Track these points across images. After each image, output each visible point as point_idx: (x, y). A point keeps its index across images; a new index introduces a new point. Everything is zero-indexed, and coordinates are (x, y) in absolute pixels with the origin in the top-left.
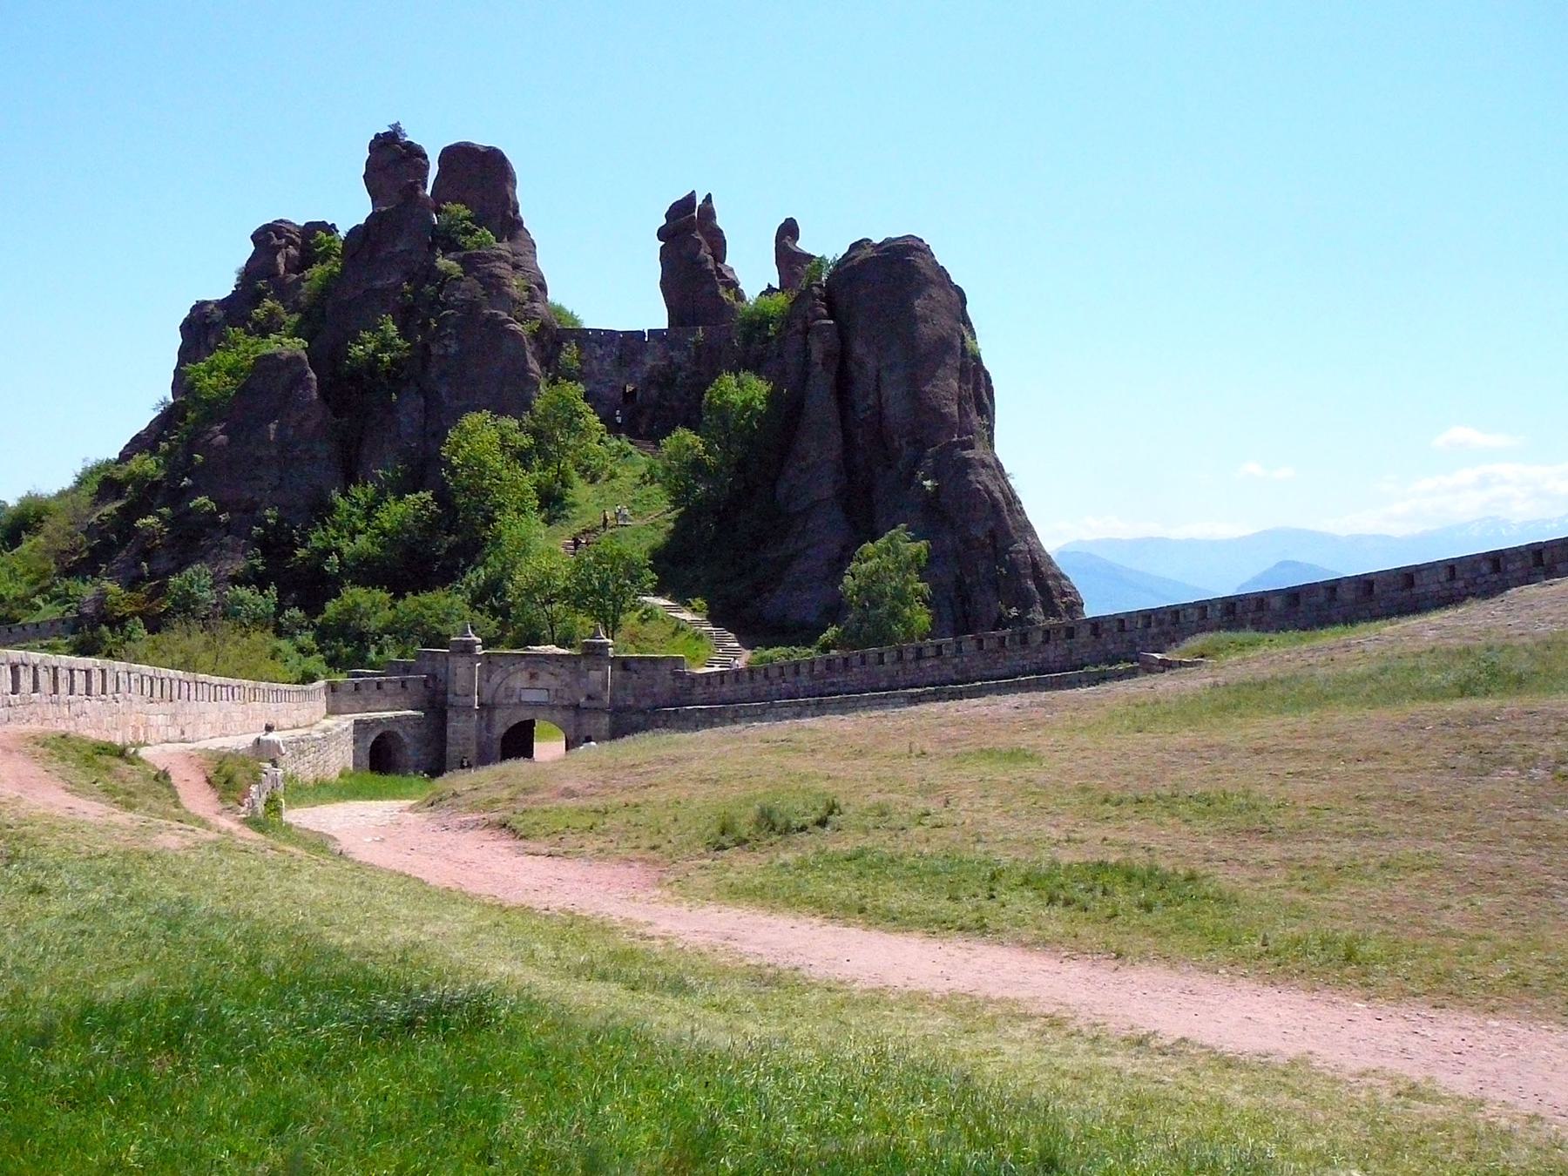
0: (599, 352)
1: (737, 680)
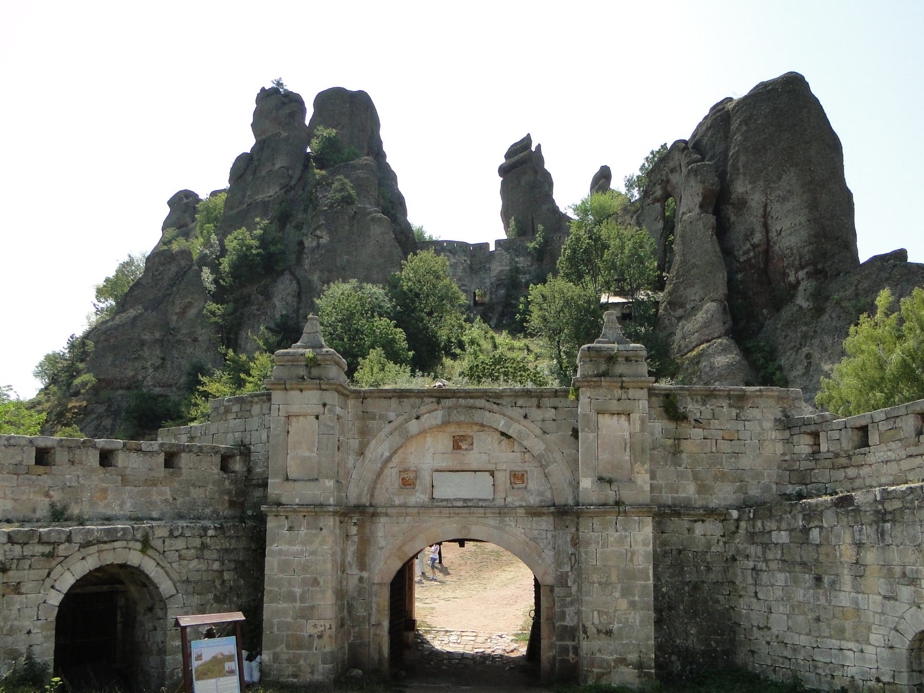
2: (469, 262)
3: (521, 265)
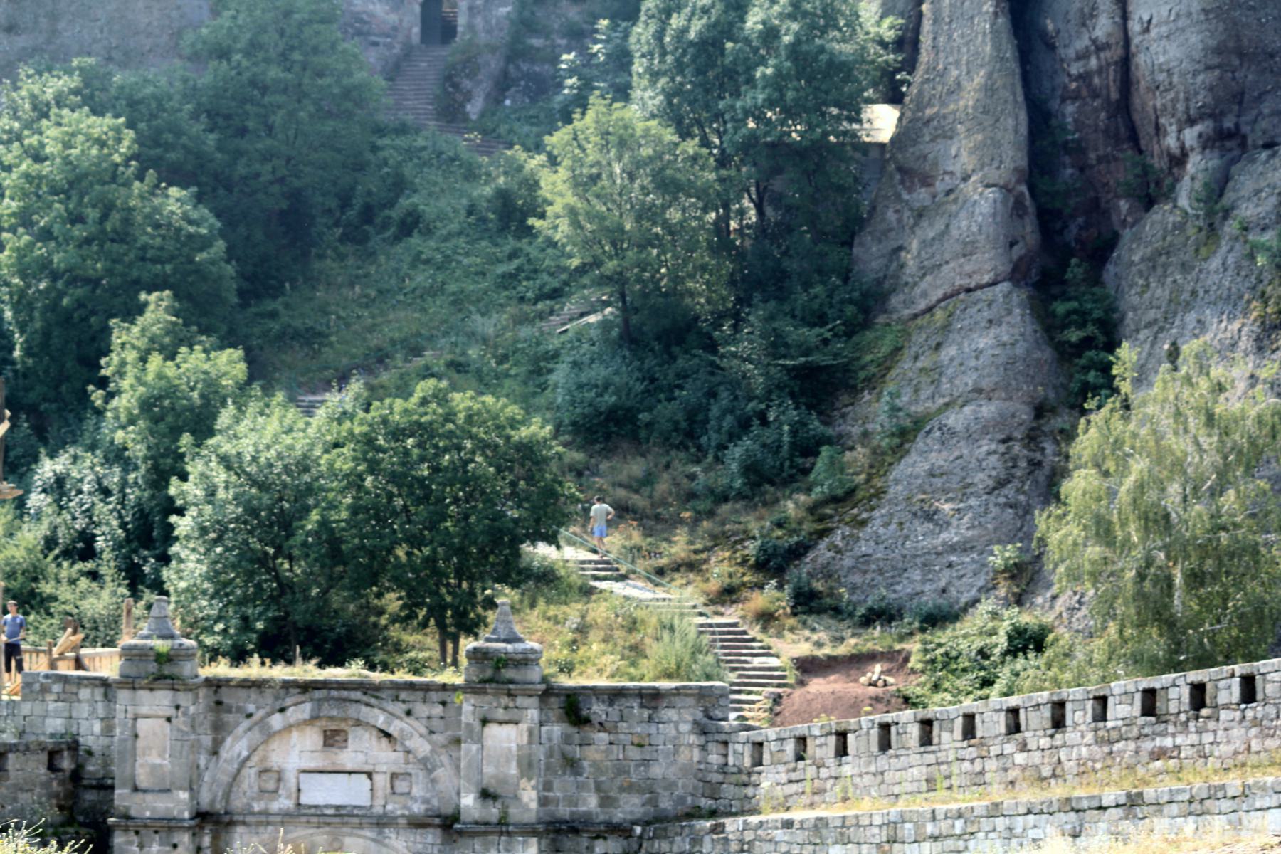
1: (885, 745)
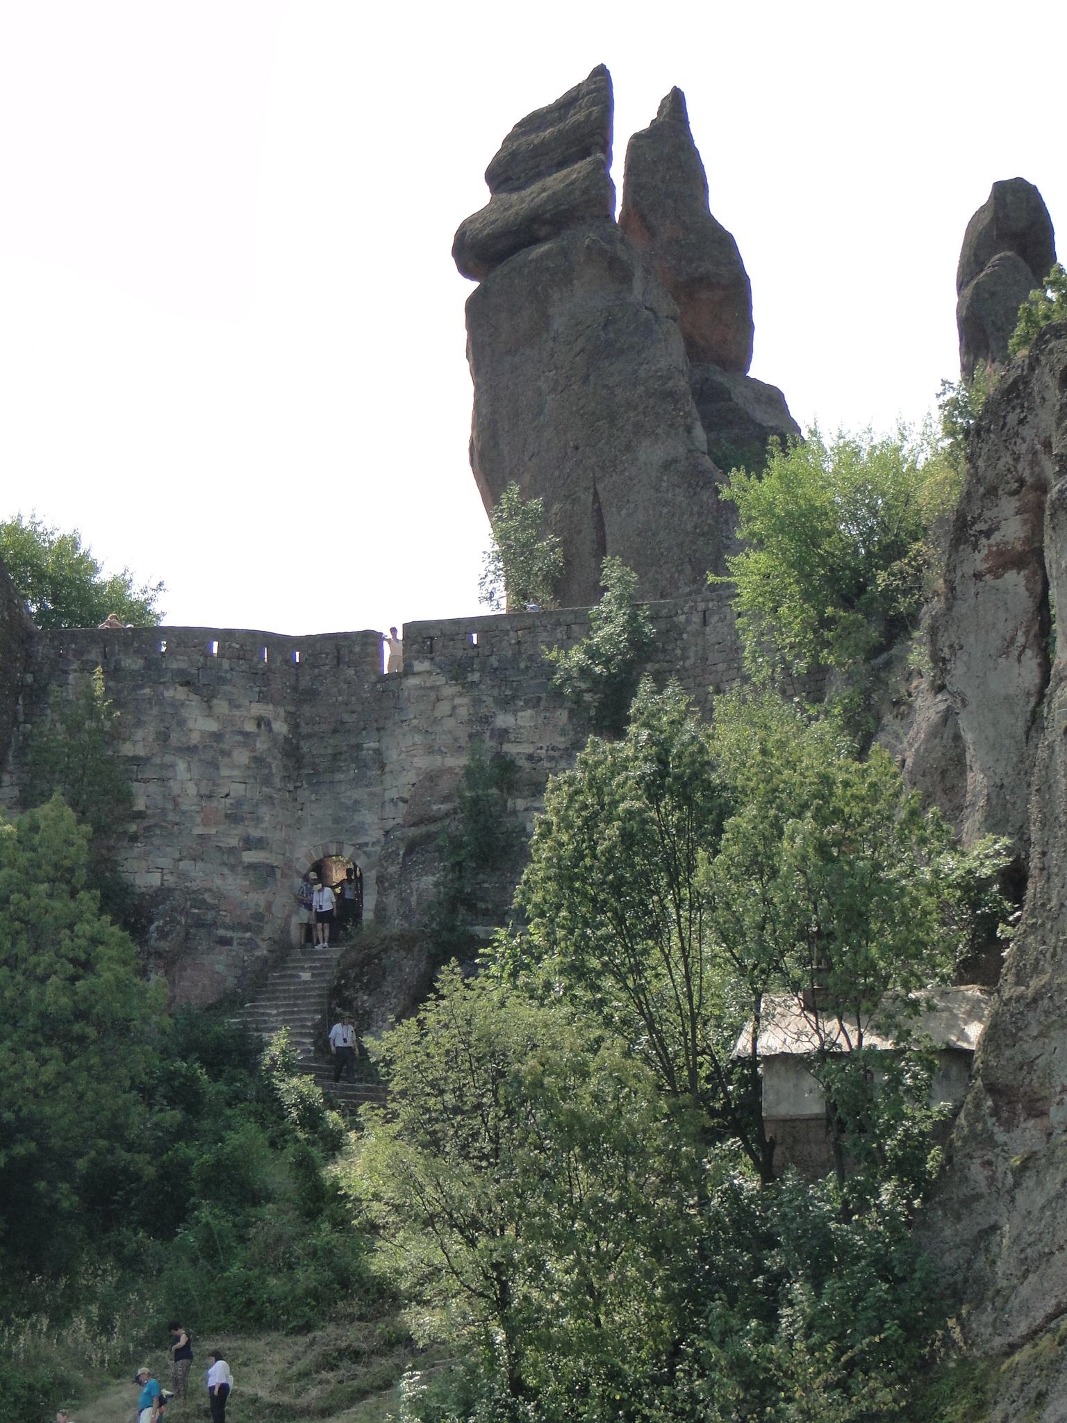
0: (200, 724)
2: (280, 727)
3: (529, 749)
